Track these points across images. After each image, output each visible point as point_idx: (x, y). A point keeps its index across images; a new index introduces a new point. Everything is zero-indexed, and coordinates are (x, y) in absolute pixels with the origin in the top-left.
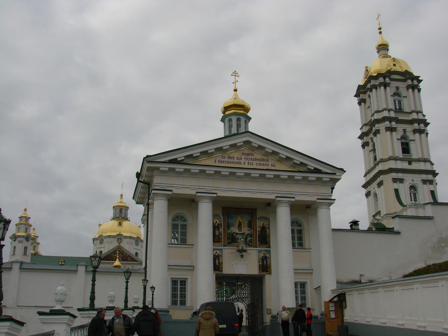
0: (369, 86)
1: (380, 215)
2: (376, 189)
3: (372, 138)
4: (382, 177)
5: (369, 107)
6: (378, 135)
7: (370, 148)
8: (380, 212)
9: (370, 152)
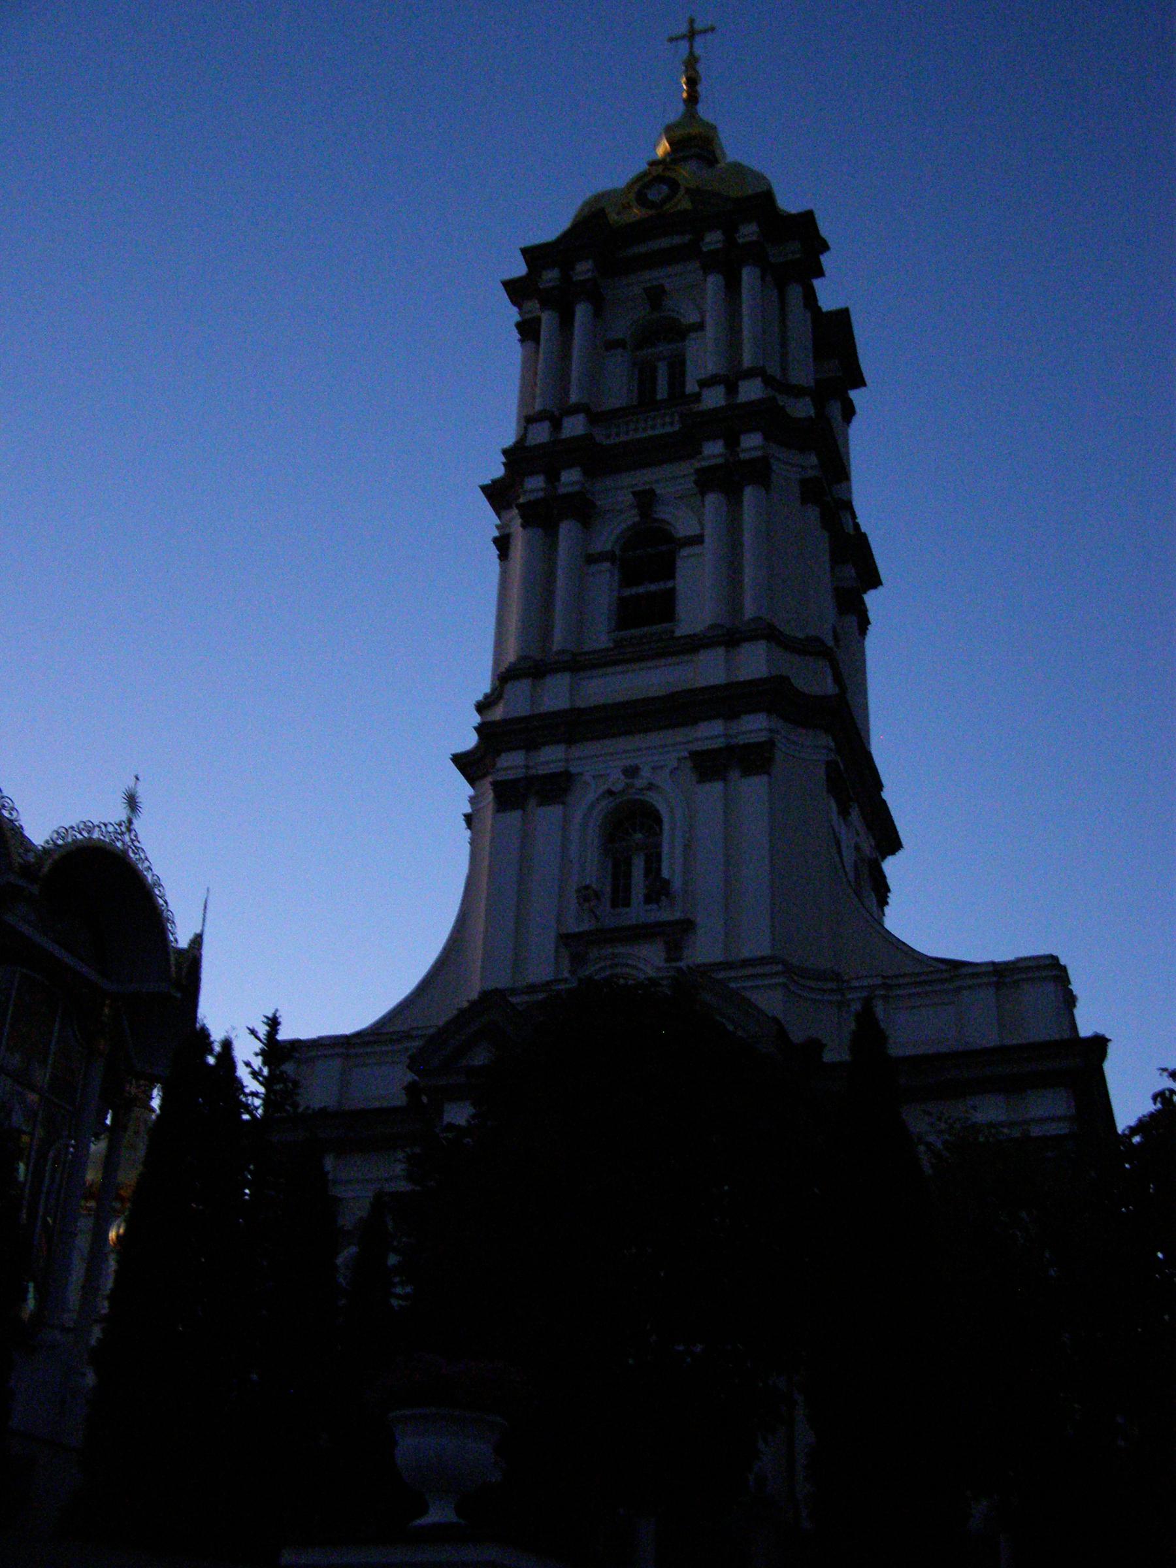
0: (713, 240)
1: (674, 949)
2: (646, 772)
3: (646, 500)
4: (754, 726)
5: (620, 344)
6: (750, 494)
7: (606, 537)
8: (687, 926)
9: (591, 559)
